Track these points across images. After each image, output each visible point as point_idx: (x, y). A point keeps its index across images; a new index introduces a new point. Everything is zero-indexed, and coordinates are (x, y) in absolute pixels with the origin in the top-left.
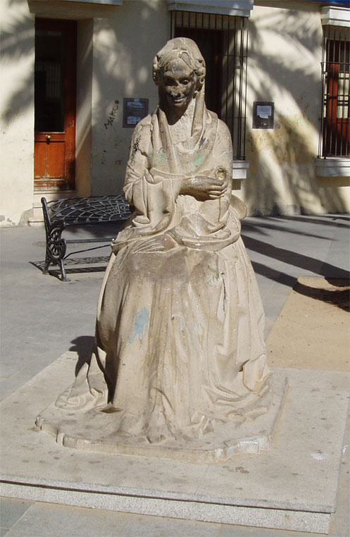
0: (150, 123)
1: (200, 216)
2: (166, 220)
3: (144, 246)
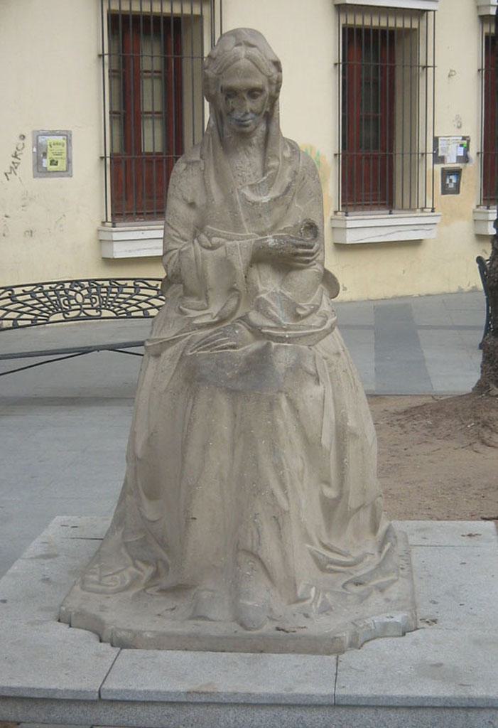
0: (198, 158)
1: (283, 294)
2: (233, 303)
3: (206, 343)
